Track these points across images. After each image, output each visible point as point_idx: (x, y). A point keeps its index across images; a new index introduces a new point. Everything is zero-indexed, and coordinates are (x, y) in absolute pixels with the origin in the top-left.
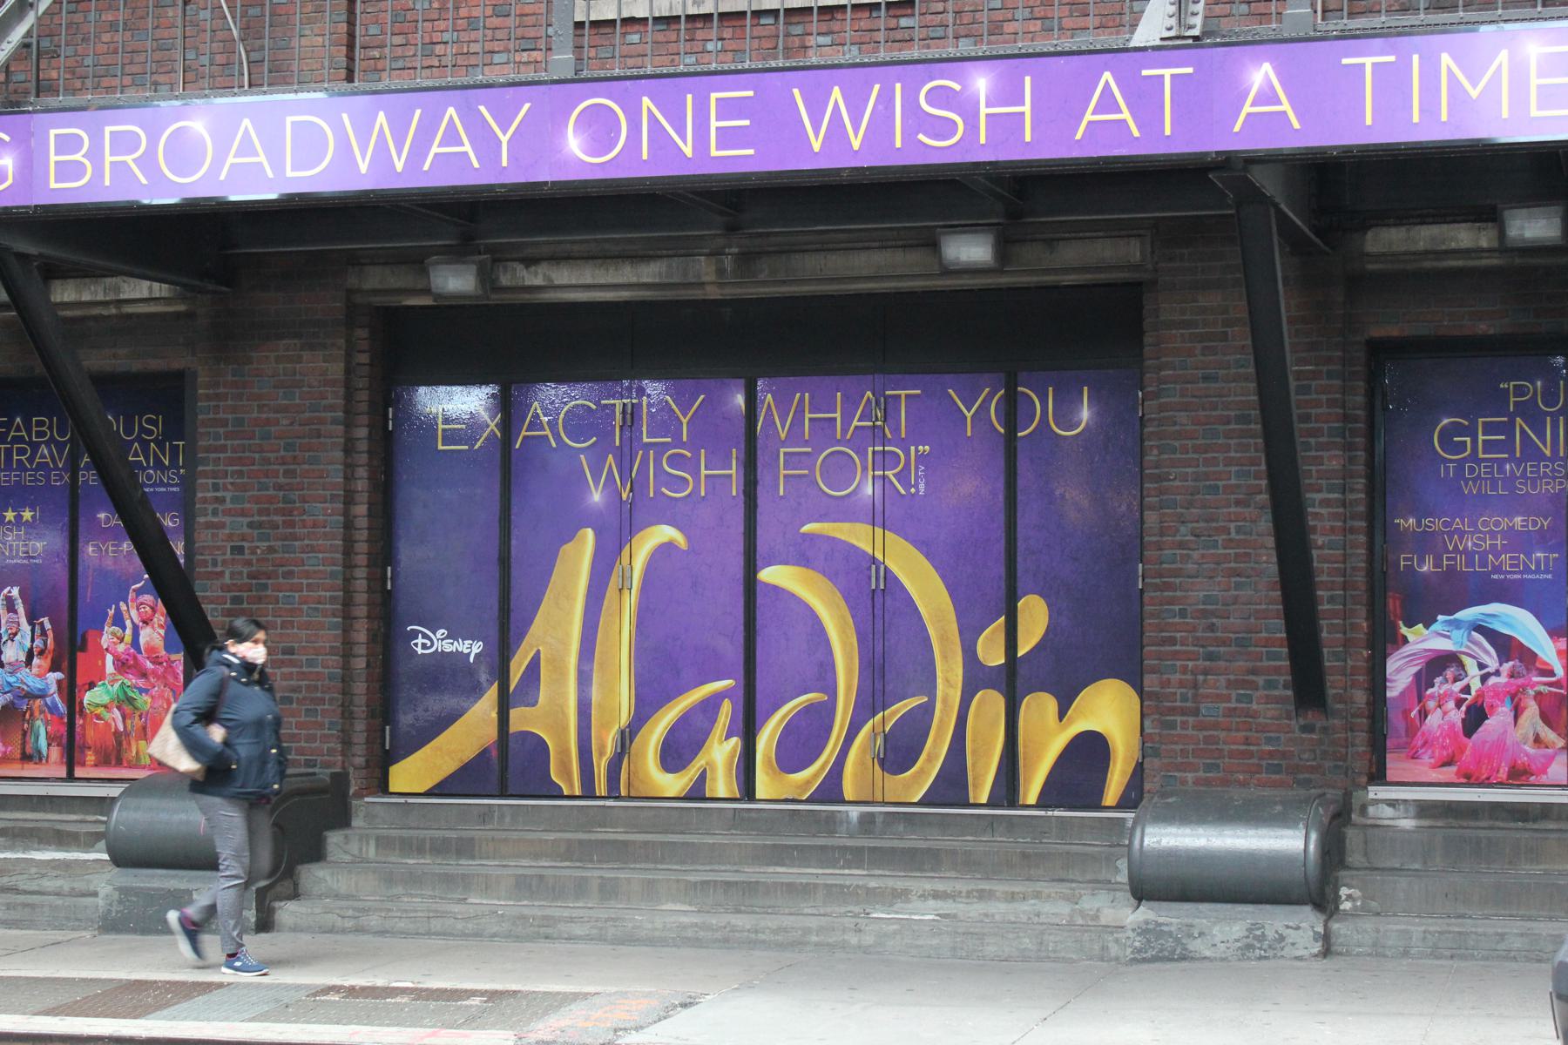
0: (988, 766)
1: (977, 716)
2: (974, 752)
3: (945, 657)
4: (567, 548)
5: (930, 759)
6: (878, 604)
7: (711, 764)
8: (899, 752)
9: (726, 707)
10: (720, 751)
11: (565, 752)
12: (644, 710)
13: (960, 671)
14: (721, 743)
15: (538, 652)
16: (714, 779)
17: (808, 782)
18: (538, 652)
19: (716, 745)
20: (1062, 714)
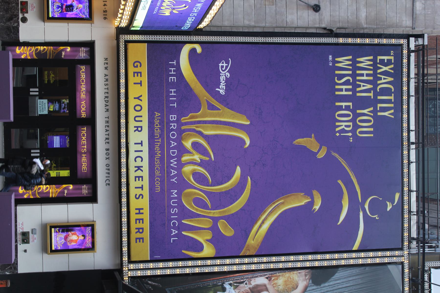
0: (195, 223)
1: (207, 220)
2: (198, 220)
3: (220, 212)
4: (245, 117)
5: (196, 210)
6: (233, 195)
7: (194, 155)
8: (199, 202)
9: (207, 159)
10: (197, 157)
11: (197, 117)
12: (207, 138)
13: (217, 216)
14: (199, 157)
15: (220, 110)
16: (190, 156)
17: (190, 180)
18: (220, 110)
19: (199, 156)
20: (208, 240)
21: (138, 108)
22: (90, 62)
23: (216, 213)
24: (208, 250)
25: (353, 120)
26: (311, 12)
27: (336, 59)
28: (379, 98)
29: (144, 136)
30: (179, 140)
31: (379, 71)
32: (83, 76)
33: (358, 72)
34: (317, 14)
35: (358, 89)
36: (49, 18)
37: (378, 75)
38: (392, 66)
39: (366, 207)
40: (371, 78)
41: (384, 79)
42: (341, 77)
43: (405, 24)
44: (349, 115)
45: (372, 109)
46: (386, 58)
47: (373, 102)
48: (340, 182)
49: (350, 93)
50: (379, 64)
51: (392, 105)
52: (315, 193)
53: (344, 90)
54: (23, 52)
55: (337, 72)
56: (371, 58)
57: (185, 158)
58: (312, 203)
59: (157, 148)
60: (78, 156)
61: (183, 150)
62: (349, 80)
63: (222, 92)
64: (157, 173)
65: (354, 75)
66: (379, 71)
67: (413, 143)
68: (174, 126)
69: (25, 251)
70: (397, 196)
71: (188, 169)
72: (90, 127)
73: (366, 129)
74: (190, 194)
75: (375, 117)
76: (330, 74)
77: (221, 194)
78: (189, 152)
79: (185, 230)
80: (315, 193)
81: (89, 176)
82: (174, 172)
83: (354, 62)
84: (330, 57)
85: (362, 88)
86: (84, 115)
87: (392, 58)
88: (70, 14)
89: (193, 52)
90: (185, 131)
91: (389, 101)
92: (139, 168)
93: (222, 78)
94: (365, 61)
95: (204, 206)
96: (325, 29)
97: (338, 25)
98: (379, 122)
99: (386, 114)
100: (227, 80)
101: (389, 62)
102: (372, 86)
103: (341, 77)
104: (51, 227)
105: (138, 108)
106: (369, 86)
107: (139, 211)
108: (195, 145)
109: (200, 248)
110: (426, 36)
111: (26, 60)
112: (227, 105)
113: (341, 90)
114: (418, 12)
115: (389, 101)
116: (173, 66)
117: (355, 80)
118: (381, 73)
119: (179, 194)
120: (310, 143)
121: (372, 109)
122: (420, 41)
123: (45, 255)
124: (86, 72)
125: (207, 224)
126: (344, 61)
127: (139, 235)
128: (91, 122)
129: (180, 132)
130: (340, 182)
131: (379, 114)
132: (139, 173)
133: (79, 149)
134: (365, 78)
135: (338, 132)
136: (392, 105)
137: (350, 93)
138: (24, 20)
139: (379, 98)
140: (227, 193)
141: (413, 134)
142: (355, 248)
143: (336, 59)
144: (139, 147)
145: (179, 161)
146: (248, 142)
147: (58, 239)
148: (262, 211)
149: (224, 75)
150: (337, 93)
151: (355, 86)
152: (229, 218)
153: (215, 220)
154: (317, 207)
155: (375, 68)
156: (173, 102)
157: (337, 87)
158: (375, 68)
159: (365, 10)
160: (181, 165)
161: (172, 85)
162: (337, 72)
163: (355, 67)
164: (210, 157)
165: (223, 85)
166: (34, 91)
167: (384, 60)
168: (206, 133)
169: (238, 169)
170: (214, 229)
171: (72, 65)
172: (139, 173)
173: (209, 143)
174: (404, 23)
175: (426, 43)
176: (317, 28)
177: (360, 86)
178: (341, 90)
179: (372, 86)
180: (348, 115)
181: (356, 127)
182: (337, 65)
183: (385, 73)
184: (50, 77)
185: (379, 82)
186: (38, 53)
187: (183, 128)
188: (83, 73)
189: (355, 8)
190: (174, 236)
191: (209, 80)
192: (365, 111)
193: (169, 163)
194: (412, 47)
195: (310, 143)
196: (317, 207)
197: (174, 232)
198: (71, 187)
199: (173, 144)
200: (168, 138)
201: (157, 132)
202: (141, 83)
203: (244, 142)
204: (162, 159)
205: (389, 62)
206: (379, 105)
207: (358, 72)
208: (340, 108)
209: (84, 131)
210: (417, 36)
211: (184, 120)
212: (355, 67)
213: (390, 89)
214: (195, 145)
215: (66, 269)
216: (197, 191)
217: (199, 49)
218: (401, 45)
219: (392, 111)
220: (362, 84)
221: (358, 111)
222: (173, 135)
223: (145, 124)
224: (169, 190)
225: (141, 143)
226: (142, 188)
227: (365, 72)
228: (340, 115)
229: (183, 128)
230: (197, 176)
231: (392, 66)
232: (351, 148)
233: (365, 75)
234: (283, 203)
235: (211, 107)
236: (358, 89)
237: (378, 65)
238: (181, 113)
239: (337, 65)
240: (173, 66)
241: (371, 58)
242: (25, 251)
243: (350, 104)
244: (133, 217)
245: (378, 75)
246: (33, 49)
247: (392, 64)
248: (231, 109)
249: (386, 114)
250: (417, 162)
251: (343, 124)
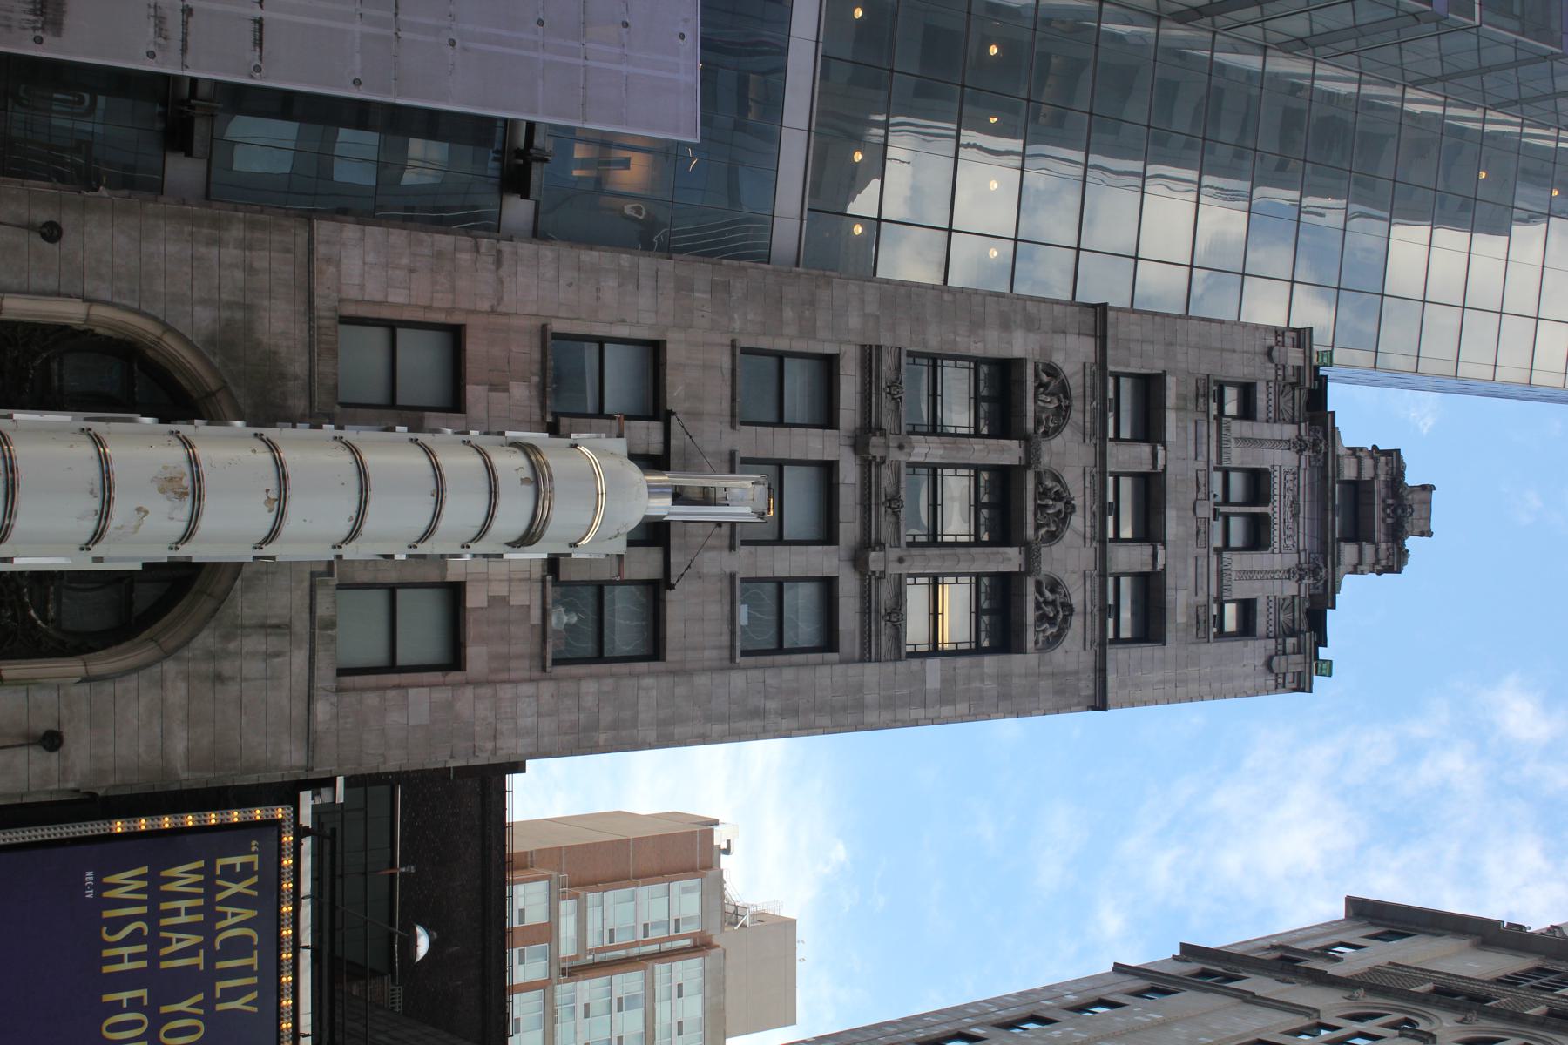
26: (37, 753)
27: (107, 880)
28: (220, 965)
31: (219, 897)
33: (164, 906)
34: (55, 755)
35: (164, 951)
37: (219, 908)
38: (255, 880)
40: (200, 918)
41: (234, 915)
42: (116, 925)
43: (291, 758)
44: (138, 1024)
45: (200, 997)
46: (237, 860)
49: (143, 964)
50: (221, 877)
51: (254, 980)
53: (125, 958)
55: (107, 914)
56: (200, 864)
62: (140, 930)
65: (153, 917)
66: (219, 897)
76: (89, 920)
83: (154, 880)
84: (89, 877)
85: (176, 947)
87: (255, 858)
94: (183, 876)
96: (77, 791)
97: (111, 781)
99: (238, 1004)
101: (247, 870)
102: (200, 939)
106: (193, 939)
110: (340, 781)
113: (119, 959)
114: (320, 728)
117: (155, 928)
118: (225, 902)
121: (200, 997)
122: (326, 795)
126: (127, 883)
131: (220, 1007)
134: (183, 919)
136: (254, 980)
137: (143, 964)
139: (220, 965)
143: (107, 880)
150: (106, 969)
151: (156, 942)
155: (209, 886)
157: (107, 953)
159: (185, 735)
162: (107, 914)
163: (155, 894)
167: (234, 865)
174: (286, 757)
175: (340, 799)
176: (51, 793)
177: (168, 942)
178: (119, 959)
179: (200, 939)
180: (138, 1024)
182: (106, 894)
183: (238, 900)
185: (219, 925)
189: (158, 730)
192: (183, 1006)
194: (306, 819)
206: (220, 985)
207: (164, 906)
208: (116, 1007)
210: (319, 784)
212: (155, 894)
213: (250, 939)
218: (277, 824)
219: (254, 995)
220: (175, 936)
221: (164, 1009)
227: (182, 904)
231: (255, 880)
233: (183, 912)
236: (164, 951)
237: (219, 882)
239: (106, 894)
241: (200, 864)
243: (143, 993)
245: (219, 908)
247: (254, 874)
249: (238, 1004)
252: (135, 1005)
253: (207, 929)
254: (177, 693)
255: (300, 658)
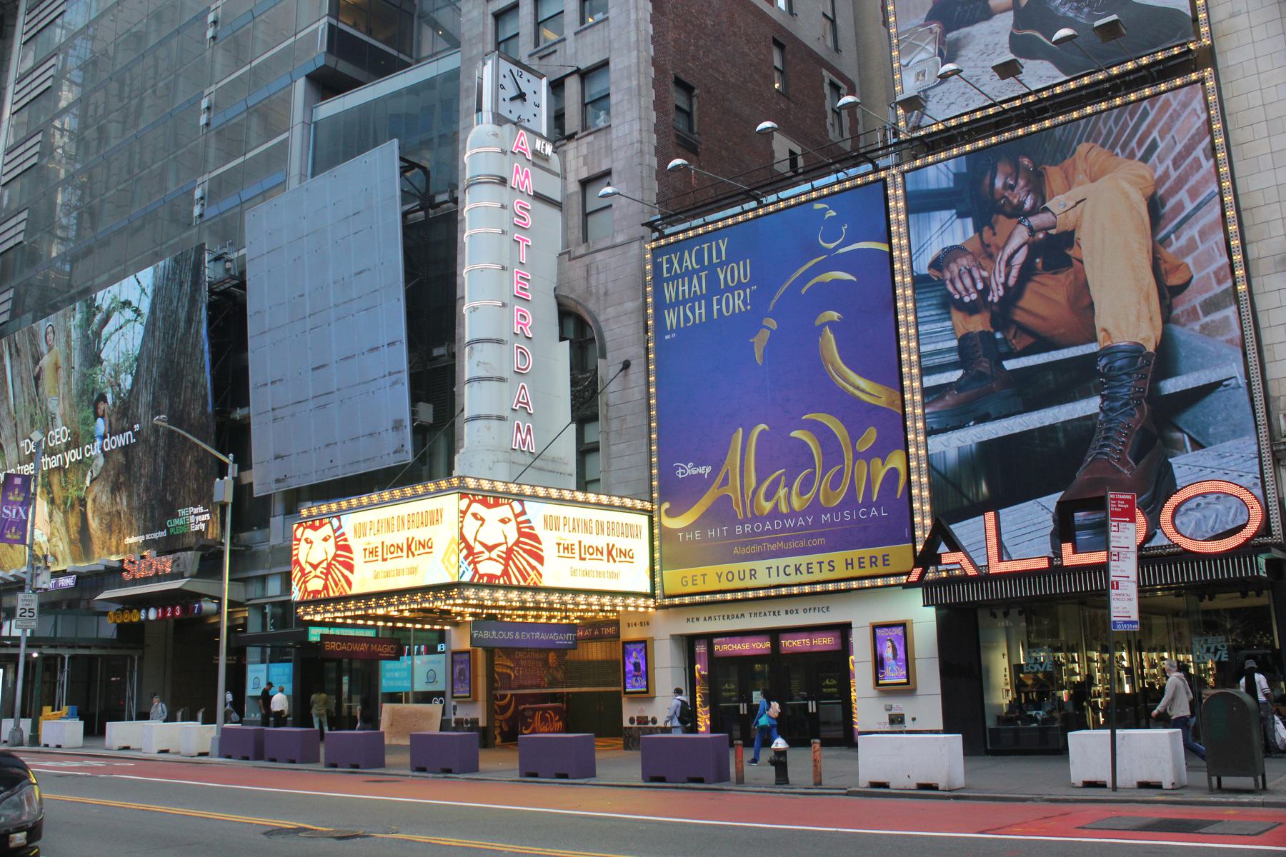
8: (835, 483)
10: (782, 492)
12: (759, 482)
21: (730, 577)
22: (709, 638)
23: (848, 457)
24: (896, 461)
25: (732, 290)
26: (632, 369)
29: (760, 565)
30: (763, 519)
32: (725, 647)
36: (647, 692)
39: (832, 246)
42: (687, 319)
46: (665, 266)
47: (712, 269)
48: (804, 291)
52: (818, 323)
54: (704, 721)
57: (784, 508)
58: (831, 324)
59: (773, 547)
60: (815, 649)
61: (775, 512)
63: (708, 469)
64: (802, 544)
65: (684, 302)
67: (759, 202)
68: (748, 529)
69: (914, 719)
70: (817, 206)
71: (797, 503)
72: (781, 636)
73: (741, 271)
74: (827, 497)
75: (727, 263)
77: (825, 453)
78: (776, 505)
79: (871, 498)
80: (818, 323)
81: (838, 634)
82: (801, 522)
84: (667, 337)
86: (768, 645)
88: (643, 667)
89: (669, 513)
90: (752, 512)
91: (710, 248)
92: (797, 569)
93: (694, 472)
94: (669, 292)
95: (840, 474)
98: (733, 257)
99: (723, 249)
100: (696, 466)
103: (687, 319)
104: (877, 684)
105: (730, 577)
106: (695, 280)
107: (849, 564)
108: (768, 497)
109: (893, 473)
111: (711, 719)
112: (722, 461)
115: (710, 248)
116: (684, 537)
119: (826, 510)
120: (760, 341)
123: (919, 691)
124: (721, 644)
125: (862, 466)
126: (671, 319)
127: (880, 562)
128: (774, 634)
129: (755, 518)
130: (804, 291)
132: (803, 568)
133: (806, 650)
134: (686, 288)
135: (745, 306)
138: (654, 721)
140: (822, 445)
141: (746, 206)
142: (885, 248)
144: (774, 571)
145: (787, 516)
146: (763, 426)
147: (894, 674)
148: (843, 392)
149: (691, 470)
152: (854, 437)
153: (857, 456)
154: (834, 315)
155: (677, 276)
156: (722, 531)
158: (677, 276)
160: (793, 514)
161: (704, 535)
164: (780, 475)
165: (701, 470)
166: (743, 709)
168: (754, 484)
169: (796, 434)
170: (868, 456)
171: (716, 662)
172: (803, 568)
173: (765, 479)
181: (740, 286)
183: (680, 263)
184: (729, 688)
186: (704, 704)
187: (749, 515)
188: (723, 647)
190: (879, 512)
191: (697, 487)
192: (722, 277)
193: (790, 529)
195: (760, 341)
196: (834, 315)
197: (874, 512)
198: (698, 666)
199: (768, 526)
200: (761, 534)
201: (755, 549)
202: (704, 575)
203: (763, 432)
204: (786, 540)
205: (670, 261)
206: (715, 261)
208: (720, 311)
209: (791, 644)
211: (740, 516)
214: (768, 497)
215: (937, 661)
216: (822, 485)
217: (666, 505)
222: (758, 527)
223: (747, 566)
224: (823, 526)
225: (769, 568)
226: (820, 563)
228: (728, 310)
229: (749, 515)
230: (806, 487)
232: (762, 283)
234: (833, 365)
235: (725, 482)
238: (732, 519)
240: (684, 537)
242: (914, 719)
244: (857, 572)
246: (699, 710)
248: (726, 455)
249: (723, 249)
250: (776, 191)
251: (737, 302)
252: (719, 302)
253: (689, 274)
254: (611, 311)
255: (599, 256)
